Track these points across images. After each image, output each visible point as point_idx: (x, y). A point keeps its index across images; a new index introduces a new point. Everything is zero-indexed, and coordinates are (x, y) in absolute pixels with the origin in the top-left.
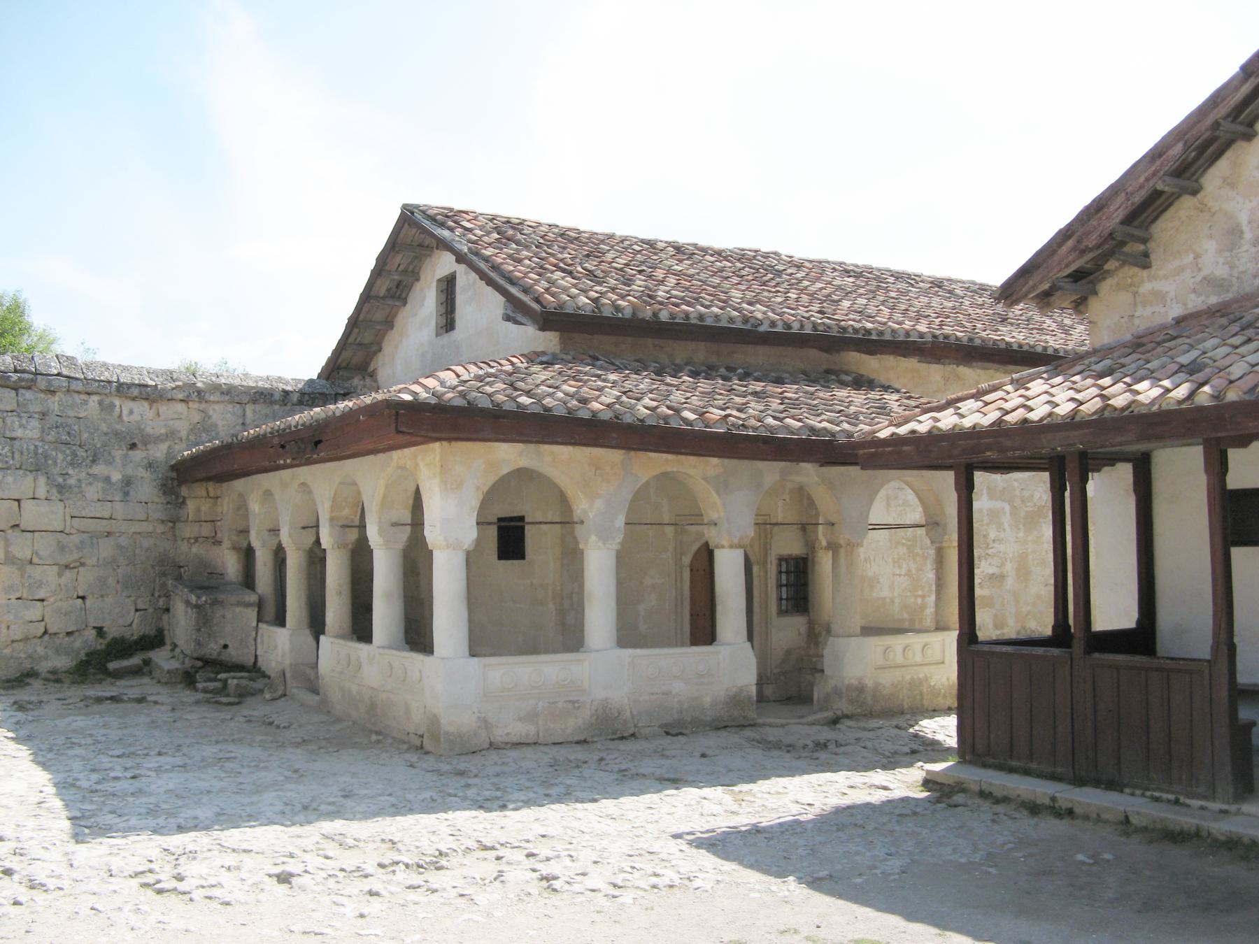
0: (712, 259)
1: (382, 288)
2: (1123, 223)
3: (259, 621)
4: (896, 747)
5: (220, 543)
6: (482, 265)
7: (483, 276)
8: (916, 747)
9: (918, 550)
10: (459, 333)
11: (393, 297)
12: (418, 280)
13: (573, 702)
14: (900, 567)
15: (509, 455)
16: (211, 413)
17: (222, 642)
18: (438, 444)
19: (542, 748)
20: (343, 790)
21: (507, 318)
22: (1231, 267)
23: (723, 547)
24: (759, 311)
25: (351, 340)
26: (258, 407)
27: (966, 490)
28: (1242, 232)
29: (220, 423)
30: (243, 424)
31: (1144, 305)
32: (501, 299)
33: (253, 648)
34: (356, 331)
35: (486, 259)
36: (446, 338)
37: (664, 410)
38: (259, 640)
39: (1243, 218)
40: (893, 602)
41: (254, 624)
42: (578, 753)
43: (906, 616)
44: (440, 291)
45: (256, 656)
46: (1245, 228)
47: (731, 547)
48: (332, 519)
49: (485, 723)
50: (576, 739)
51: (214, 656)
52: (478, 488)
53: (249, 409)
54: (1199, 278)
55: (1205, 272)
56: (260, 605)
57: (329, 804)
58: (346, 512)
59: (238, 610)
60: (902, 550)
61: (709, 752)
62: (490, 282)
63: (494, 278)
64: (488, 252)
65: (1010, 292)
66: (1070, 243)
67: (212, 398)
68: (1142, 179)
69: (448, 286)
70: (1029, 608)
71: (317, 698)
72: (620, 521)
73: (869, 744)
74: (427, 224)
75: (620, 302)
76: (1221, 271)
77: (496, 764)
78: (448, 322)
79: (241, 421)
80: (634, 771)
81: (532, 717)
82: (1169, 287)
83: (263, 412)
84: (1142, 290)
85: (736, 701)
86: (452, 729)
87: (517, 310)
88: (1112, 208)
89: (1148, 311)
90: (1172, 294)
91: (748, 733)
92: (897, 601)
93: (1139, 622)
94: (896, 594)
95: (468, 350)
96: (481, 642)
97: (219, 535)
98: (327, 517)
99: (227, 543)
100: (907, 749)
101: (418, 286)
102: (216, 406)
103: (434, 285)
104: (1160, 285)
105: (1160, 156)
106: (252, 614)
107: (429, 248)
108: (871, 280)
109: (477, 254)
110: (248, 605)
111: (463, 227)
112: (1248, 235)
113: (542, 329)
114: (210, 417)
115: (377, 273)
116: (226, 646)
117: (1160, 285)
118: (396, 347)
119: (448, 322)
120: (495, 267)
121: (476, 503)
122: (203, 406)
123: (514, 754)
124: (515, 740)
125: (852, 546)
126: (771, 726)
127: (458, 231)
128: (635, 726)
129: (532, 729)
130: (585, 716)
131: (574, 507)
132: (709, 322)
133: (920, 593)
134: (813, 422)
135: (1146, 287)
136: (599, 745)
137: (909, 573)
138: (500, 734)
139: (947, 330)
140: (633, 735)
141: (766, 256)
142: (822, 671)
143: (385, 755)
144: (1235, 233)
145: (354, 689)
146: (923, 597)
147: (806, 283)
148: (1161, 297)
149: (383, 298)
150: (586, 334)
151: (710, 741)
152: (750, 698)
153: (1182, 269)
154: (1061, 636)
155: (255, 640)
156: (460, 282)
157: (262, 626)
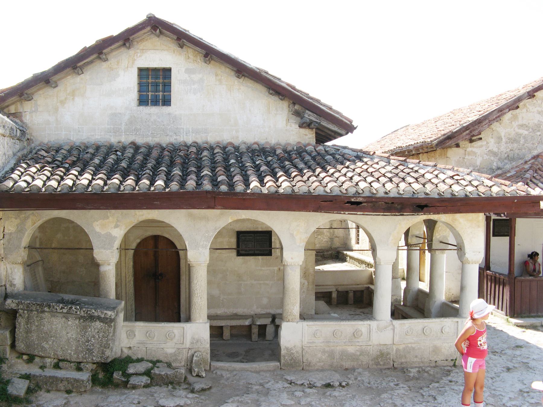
31: (469, 154)
39: (503, 135)
46: (503, 137)
54: (488, 150)
55: (490, 149)
66: (468, 132)
68: (494, 117)
76: (495, 150)
82: (478, 151)
88: (483, 124)
89: (470, 157)
90: (479, 153)
101: (105, 65)
104: (474, 150)
105: (501, 111)
112: (504, 140)
117: (474, 150)
118: (62, 103)
144: (500, 138)
148: (475, 153)
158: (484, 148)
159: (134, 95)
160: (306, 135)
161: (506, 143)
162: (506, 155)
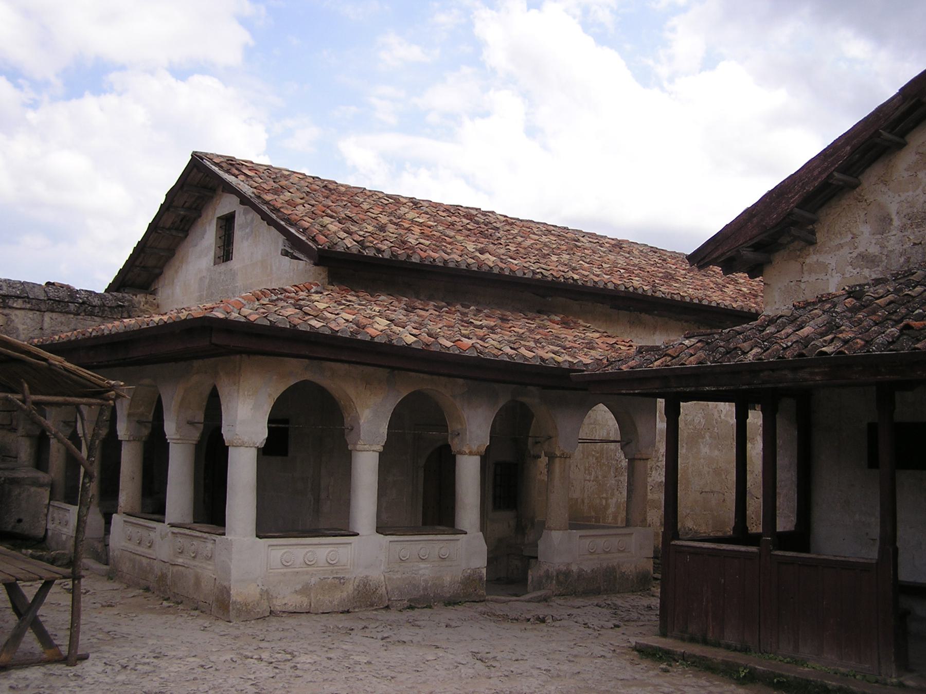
0: (444, 214)
1: (168, 221)
2: (799, 206)
3: (50, 500)
4: (602, 623)
5: (14, 430)
6: (265, 208)
7: (265, 217)
8: (617, 623)
9: (604, 461)
10: (235, 263)
11: (177, 229)
12: (200, 216)
13: (340, 579)
14: (590, 474)
15: (297, 372)
16: (13, 318)
17: (17, 518)
18: (238, 357)
19: (315, 617)
20: (153, 651)
21: (285, 253)
22: (882, 247)
23: (465, 454)
24: (489, 260)
25: (137, 263)
26: (54, 315)
27: (673, 414)
28: (891, 220)
29: (21, 327)
30: (41, 329)
32: (281, 238)
33: (44, 522)
34: (142, 255)
35: (267, 203)
36: (223, 267)
37: (425, 337)
38: (50, 517)
39: (893, 208)
40: (583, 502)
41: (47, 502)
42: (344, 622)
43: (593, 514)
44: (219, 227)
45: (47, 530)
47: (471, 453)
48: (129, 415)
49: (266, 594)
50: (341, 609)
51: (9, 528)
52: (270, 395)
53: (47, 317)
54: (854, 255)
55: (861, 249)
56: (52, 486)
57: (145, 664)
58: (142, 409)
59: (33, 489)
60: (592, 460)
61: (454, 624)
62: (271, 222)
63: (272, 218)
64: (268, 197)
65: (701, 258)
66: (755, 220)
67: (15, 305)
69: (227, 222)
70: (688, 511)
71: (105, 567)
72: (384, 430)
73: (580, 620)
74: (216, 169)
75: (380, 245)
76: (874, 250)
77: (278, 629)
78: (225, 252)
79: (39, 326)
80: (395, 638)
81: (305, 590)
82: (831, 260)
83: (59, 320)
84: (807, 261)
85: (470, 581)
86: (239, 599)
87: (295, 246)
89: (813, 278)
91: (480, 607)
92: (586, 501)
93: (797, 525)
94: (586, 496)
95: (246, 278)
96: (269, 525)
97: (14, 423)
98: (126, 413)
99: (21, 431)
100: (610, 625)
102: (18, 312)
103: (215, 222)
104: (822, 258)
106: (46, 493)
107: (213, 190)
108: (569, 239)
109: (259, 197)
110: (41, 486)
111: (245, 174)
112: (896, 222)
113: (315, 264)
114: (12, 321)
115: (164, 208)
116: (20, 521)
118: (176, 272)
119: (225, 252)
120: (276, 210)
121: (267, 408)
122: (7, 311)
123: (292, 622)
124: (291, 609)
125: (565, 457)
126: (496, 601)
127: (242, 177)
128: (389, 600)
129: (306, 601)
130: (350, 588)
131: (346, 415)
132: (451, 265)
133: (604, 495)
134: (541, 353)
135: (812, 259)
136: (360, 615)
137: (596, 479)
138: (278, 604)
139: (636, 282)
140: (387, 607)
141: (485, 214)
142: (537, 558)
143: (180, 620)
145: (145, 561)
146: (607, 499)
147: (520, 239)
148: (824, 267)
149: (169, 229)
150: (349, 269)
151: (450, 614)
152: (481, 578)
153: (841, 246)
154: (741, 534)
155: (46, 515)
156: (239, 221)
157: (52, 503)
158: (846, 250)
159: (212, 254)
160: (320, 274)
161: (903, 228)
162: (902, 260)
